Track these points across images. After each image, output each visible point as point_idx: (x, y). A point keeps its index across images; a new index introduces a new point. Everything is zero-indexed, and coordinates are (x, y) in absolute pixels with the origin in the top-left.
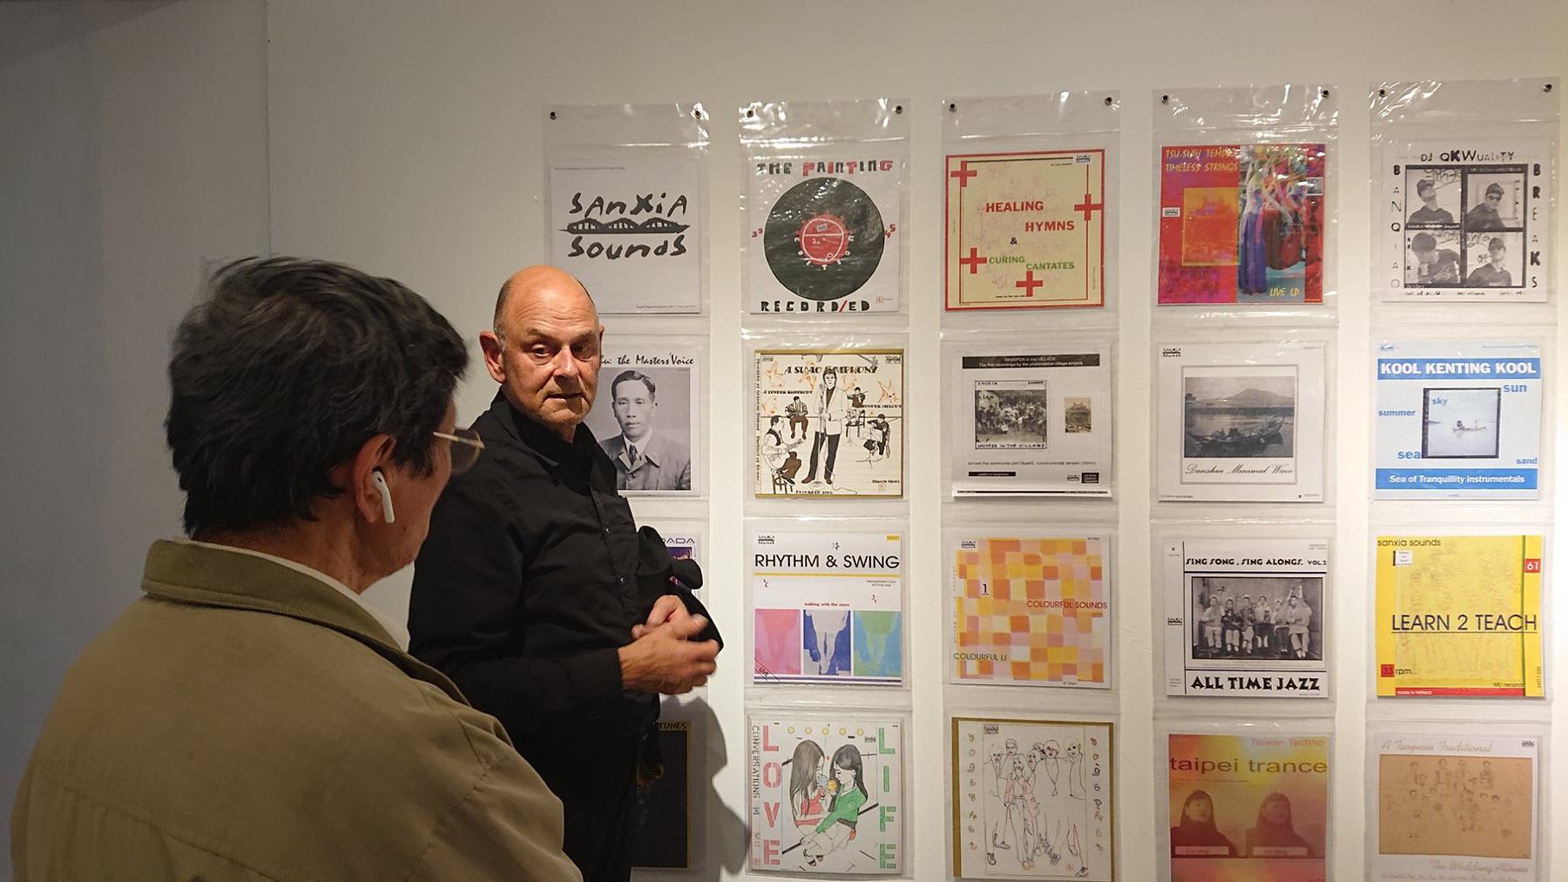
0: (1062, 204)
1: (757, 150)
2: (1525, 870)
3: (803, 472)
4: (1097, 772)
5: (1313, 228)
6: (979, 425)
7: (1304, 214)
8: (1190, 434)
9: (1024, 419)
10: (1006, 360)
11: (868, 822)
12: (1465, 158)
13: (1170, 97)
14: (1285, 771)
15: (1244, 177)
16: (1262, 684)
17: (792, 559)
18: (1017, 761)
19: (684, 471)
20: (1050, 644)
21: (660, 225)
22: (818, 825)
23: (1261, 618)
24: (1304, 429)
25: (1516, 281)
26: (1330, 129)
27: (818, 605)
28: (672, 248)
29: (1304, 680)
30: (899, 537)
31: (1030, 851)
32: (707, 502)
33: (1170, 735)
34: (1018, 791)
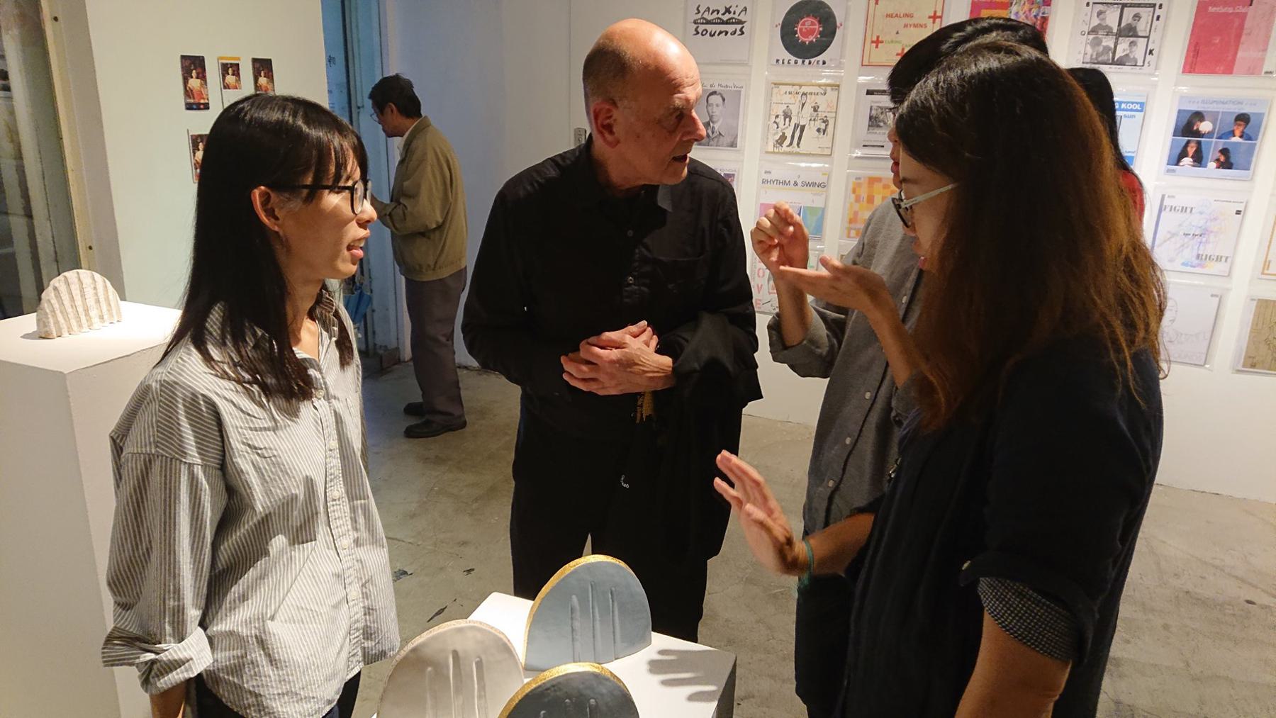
3: (787, 142)
15: (1011, 5)
21: (734, 20)
28: (738, 32)
30: (828, 174)
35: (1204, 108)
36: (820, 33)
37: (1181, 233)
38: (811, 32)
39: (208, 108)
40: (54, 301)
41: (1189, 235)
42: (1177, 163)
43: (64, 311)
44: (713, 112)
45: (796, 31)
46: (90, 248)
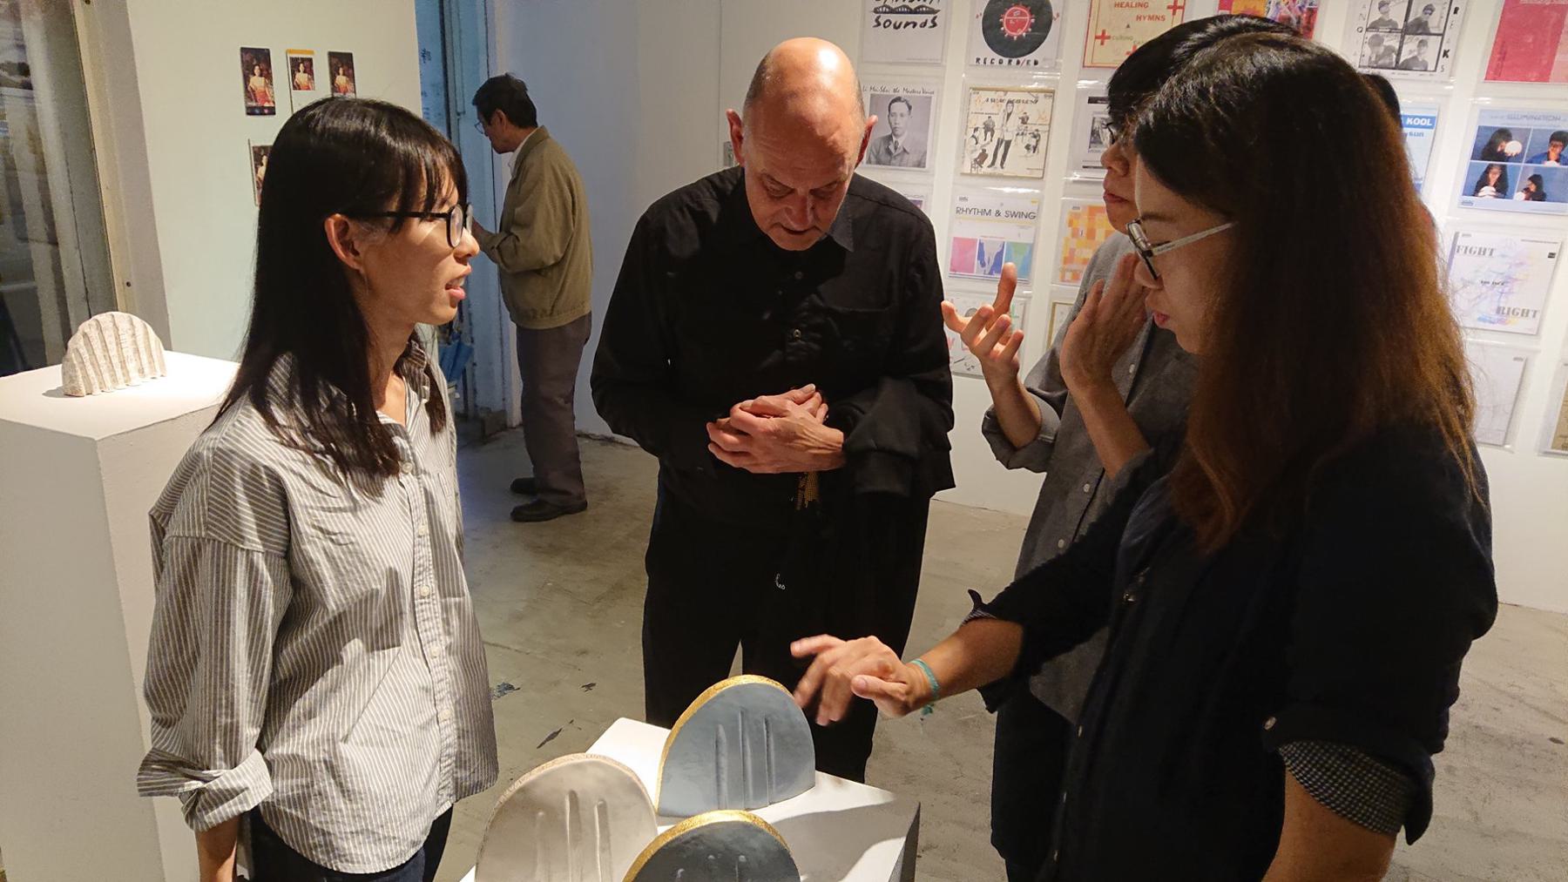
3: (989, 161)
28: (929, 24)
35: (1508, 124)
36: (1032, 26)
37: (1478, 281)
38: (1021, 25)
39: (274, 114)
40: (83, 350)
41: (1488, 283)
42: (1476, 192)
43: (95, 362)
44: (896, 124)
46: (128, 284)
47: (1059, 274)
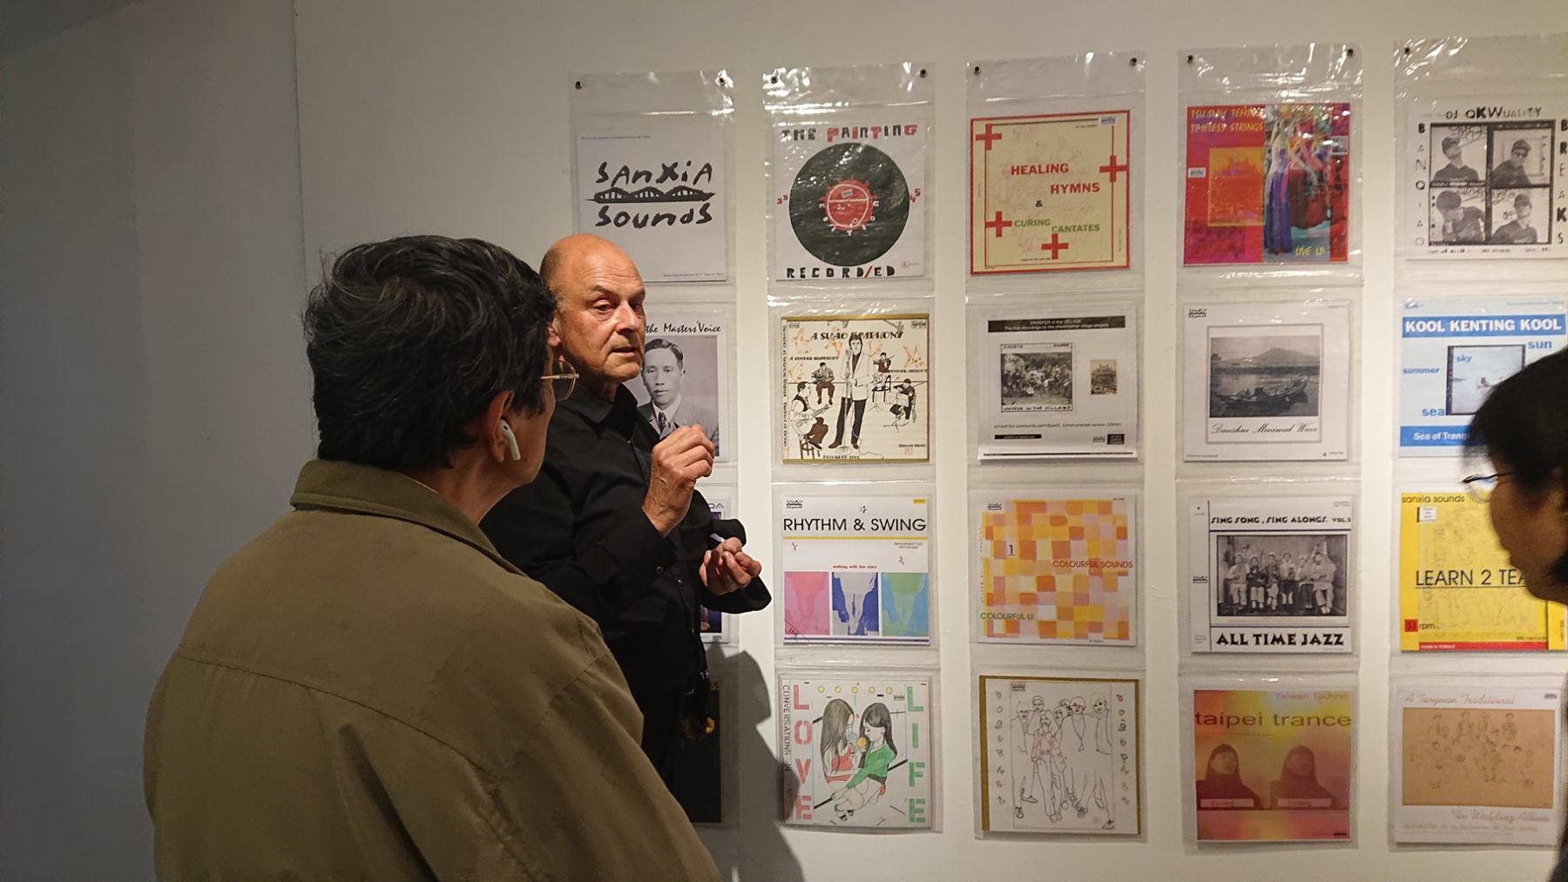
0: (1088, 166)
1: (785, 118)
2: (1545, 819)
3: (830, 437)
4: (1123, 728)
5: (1338, 187)
6: (1005, 389)
7: (1329, 174)
8: (1216, 394)
9: (1049, 382)
10: (1032, 323)
11: (897, 777)
12: (1491, 115)
13: (1196, 57)
14: (1309, 724)
15: (1269, 137)
16: (1286, 639)
17: (820, 522)
18: (1044, 718)
19: (713, 436)
20: (1075, 604)
21: (685, 193)
22: (849, 780)
23: (1285, 575)
24: (1329, 390)
25: (1542, 237)
26: (1355, 88)
27: (846, 567)
28: (697, 216)
29: (1329, 636)
30: (927, 500)
31: (1057, 805)
32: (736, 467)
33: (1196, 692)
34: (1046, 746)
36: (875, 211)
38: (856, 211)
45: (824, 210)
47: (983, 628)
